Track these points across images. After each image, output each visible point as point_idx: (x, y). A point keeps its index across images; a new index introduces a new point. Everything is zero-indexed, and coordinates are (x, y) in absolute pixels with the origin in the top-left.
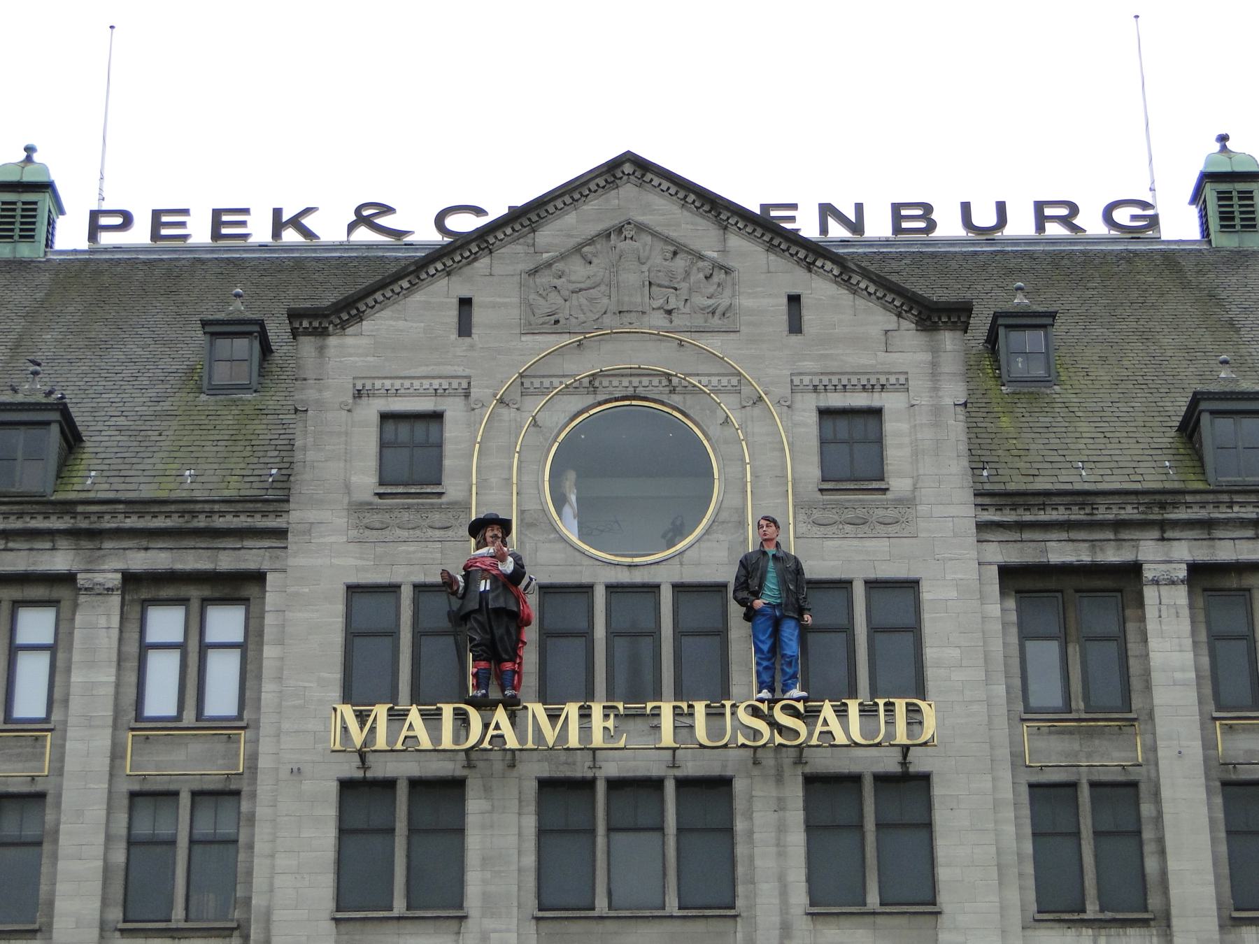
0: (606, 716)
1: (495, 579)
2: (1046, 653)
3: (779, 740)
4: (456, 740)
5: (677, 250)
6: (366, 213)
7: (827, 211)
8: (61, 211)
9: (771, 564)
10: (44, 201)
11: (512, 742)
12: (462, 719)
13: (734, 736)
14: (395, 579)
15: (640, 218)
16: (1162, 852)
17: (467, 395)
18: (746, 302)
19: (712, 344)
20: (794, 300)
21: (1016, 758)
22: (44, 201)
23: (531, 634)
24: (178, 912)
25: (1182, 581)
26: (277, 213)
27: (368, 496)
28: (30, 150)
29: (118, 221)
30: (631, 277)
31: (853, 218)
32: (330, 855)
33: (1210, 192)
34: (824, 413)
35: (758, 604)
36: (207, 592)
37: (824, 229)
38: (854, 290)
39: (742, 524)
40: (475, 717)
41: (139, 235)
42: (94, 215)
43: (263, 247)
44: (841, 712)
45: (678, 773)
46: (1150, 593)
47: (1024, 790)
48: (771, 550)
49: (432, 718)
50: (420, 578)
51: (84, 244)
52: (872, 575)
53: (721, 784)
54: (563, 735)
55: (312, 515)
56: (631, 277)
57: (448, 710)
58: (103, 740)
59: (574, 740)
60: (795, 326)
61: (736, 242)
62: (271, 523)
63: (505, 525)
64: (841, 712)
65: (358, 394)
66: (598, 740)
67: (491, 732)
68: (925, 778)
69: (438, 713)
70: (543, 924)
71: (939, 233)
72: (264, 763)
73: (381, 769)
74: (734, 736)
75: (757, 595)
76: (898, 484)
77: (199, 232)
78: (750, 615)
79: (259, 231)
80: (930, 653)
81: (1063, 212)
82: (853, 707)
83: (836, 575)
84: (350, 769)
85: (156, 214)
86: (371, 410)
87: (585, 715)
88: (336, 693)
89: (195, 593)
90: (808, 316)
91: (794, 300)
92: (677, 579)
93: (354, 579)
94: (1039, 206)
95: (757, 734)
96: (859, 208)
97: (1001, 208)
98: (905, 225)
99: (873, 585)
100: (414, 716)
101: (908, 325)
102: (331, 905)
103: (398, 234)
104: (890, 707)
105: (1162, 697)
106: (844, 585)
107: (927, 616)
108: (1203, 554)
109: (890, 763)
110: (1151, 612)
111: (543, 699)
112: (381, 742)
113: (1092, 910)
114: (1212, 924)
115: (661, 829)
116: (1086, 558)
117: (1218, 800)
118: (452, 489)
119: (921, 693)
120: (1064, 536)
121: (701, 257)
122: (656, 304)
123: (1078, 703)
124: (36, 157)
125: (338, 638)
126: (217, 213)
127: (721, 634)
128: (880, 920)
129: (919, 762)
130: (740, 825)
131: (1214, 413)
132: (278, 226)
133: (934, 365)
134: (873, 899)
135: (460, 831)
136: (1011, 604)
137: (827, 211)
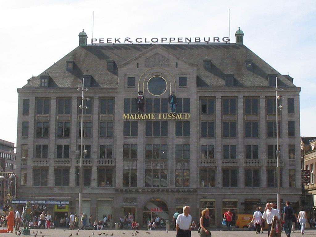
0: (153, 115)
1: (141, 99)
4: (137, 118)
6: (127, 39)
7: (186, 38)
8: (87, 37)
12: (137, 115)
14: (130, 98)
17: (138, 75)
19: (166, 69)
20: (177, 63)
21: (200, 119)
22: (86, 37)
23: (145, 105)
26: (115, 39)
28: (83, 30)
30: (157, 60)
31: (190, 40)
34: (180, 77)
35: (171, 102)
42: (92, 39)
44: (179, 115)
46: (217, 100)
47: (201, 123)
49: (134, 116)
51: (91, 44)
52: (184, 98)
54: (148, 117)
56: (157, 60)
57: (136, 114)
59: (149, 118)
60: (177, 67)
61: (170, 56)
62: (115, 91)
63: (142, 92)
64: (179, 115)
66: (152, 118)
67: (140, 117)
75: (171, 101)
76: (188, 86)
79: (113, 42)
80: (191, 107)
81: (217, 39)
82: (181, 114)
88: (123, 112)
91: (177, 63)
93: (125, 98)
97: (209, 38)
99: (184, 99)
103: (131, 42)
105: (217, 112)
106: (182, 99)
108: (223, 95)
109: (186, 121)
110: (217, 102)
111: (146, 113)
117: (223, 124)
132: (116, 41)
135: (137, 127)
136: (201, 101)
137: (186, 38)
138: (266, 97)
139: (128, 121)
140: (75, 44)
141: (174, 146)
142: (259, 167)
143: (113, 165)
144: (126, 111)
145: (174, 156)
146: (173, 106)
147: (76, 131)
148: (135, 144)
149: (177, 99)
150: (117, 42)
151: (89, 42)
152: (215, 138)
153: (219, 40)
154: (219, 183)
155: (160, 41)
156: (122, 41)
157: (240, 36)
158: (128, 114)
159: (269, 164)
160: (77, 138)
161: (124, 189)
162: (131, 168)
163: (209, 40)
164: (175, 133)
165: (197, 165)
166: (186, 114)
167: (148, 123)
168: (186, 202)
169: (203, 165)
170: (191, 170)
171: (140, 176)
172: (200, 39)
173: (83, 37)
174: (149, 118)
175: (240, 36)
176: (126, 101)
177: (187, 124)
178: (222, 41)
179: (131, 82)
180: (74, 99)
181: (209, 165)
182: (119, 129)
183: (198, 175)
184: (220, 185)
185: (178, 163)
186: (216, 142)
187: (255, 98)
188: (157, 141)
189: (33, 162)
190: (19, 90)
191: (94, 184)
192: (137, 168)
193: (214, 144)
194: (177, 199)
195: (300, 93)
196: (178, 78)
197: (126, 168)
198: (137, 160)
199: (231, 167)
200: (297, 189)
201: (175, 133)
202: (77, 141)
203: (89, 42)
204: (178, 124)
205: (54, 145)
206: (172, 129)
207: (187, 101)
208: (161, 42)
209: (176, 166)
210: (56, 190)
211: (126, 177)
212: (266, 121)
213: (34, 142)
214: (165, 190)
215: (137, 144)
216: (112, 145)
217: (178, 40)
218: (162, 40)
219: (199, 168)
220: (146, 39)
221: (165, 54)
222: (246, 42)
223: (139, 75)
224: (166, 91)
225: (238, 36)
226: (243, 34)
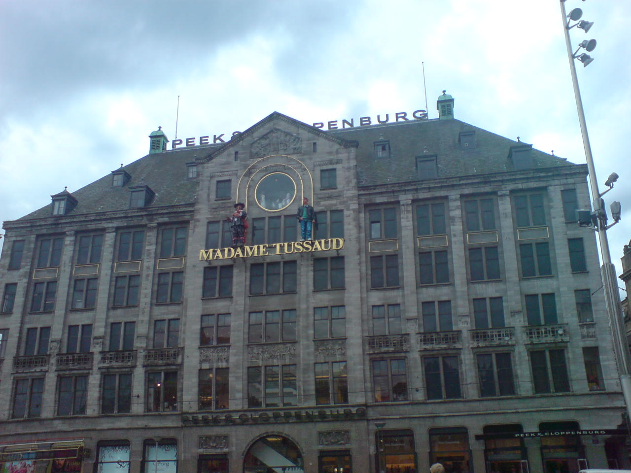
0: (264, 248)
1: (238, 217)
3: (305, 250)
7: (344, 121)
10: (162, 139)
12: (229, 250)
13: (294, 251)
15: (278, 127)
22: (162, 139)
24: (169, 300)
25: (410, 204)
26: (215, 136)
28: (160, 127)
29: (179, 142)
31: (351, 123)
36: (177, 226)
40: (233, 250)
41: (184, 145)
43: (212, 145)
44: (320, 243)
45: (284, 260)
47: (369, 258)
49: (223, 252)
53: (294, 262)
54: (253, 253)
59: (256, 254)
64: (320, 243)
66: (261, 254)
67: (237, 254)
68: (343, 258)
69: (224, 250)
70: (251, 298)
71: (372, 124)
73: (214, 264)
74: (294, 251)
77: (197, 143)
81: (403, 115)
82: (323, 241)
84: (206, 265)
85: (187, 140)
87: (259, 248)
94: (397, 114)
95: (299, 249)
96: (352, 120)
97: (387, 116)
100: (219, 251)
104: (332, 241)
109: (335, 254)
113: (385, 286)
117: (418, 258)
120: (380, 196)
122: (282, 148)
124: (161, 129)
125: (205, 234)
126: (201, 138)
127: (295, 227)
128: (331, 292)
129: (342, 253)
130: (298, 271)
131: (421, 161)
134: (329, 287)
135: (232, 277)
136: (368, 214)
137: (344, 121)
138: (512, 192)
140: (142, 149)
141: (311, 312)
142: (508, 345)
144: (209, 244)
145: (311, 332)
147: (107, 296)
149: (316, 213)
152: (402, 288)
158: (211, 250)
159: (532, 337)
160: (108, 309)
161: (200, 417)
162: (215, 366)
165: (364, 350)
166: (334, 240)
167: (256, 267)
168: (343, 440)
170: (350, 363)
171: (237, 384)
172: (371, 120)
174: (256, 254)
175: (448, 103)
177: (339, 259)
182: (193, 285)
183: (368, 373)
184: (420, 396)
186: (403, 296)
188: (274, 303)
190: (7, 225)
191: (137, 407)
192: (231, 365)
193: (399, 301)
194: (321, 434)
196: (318, 172)
197: (206, 366)
200: (609, 394)
201: (311, 283)
202: (107, 315)
204: (318, 261)
205: (61, 326)
206: (306, 276)
207: (337, 212)
210: (59, 425)
211: (204, 388)
212: (515, 242)
214: (293, 412)
215: (230, 312)
216: (178, 319)
219: (367, 358)
222: (460, 113)
225: (443, 104)
226: (452, 100)
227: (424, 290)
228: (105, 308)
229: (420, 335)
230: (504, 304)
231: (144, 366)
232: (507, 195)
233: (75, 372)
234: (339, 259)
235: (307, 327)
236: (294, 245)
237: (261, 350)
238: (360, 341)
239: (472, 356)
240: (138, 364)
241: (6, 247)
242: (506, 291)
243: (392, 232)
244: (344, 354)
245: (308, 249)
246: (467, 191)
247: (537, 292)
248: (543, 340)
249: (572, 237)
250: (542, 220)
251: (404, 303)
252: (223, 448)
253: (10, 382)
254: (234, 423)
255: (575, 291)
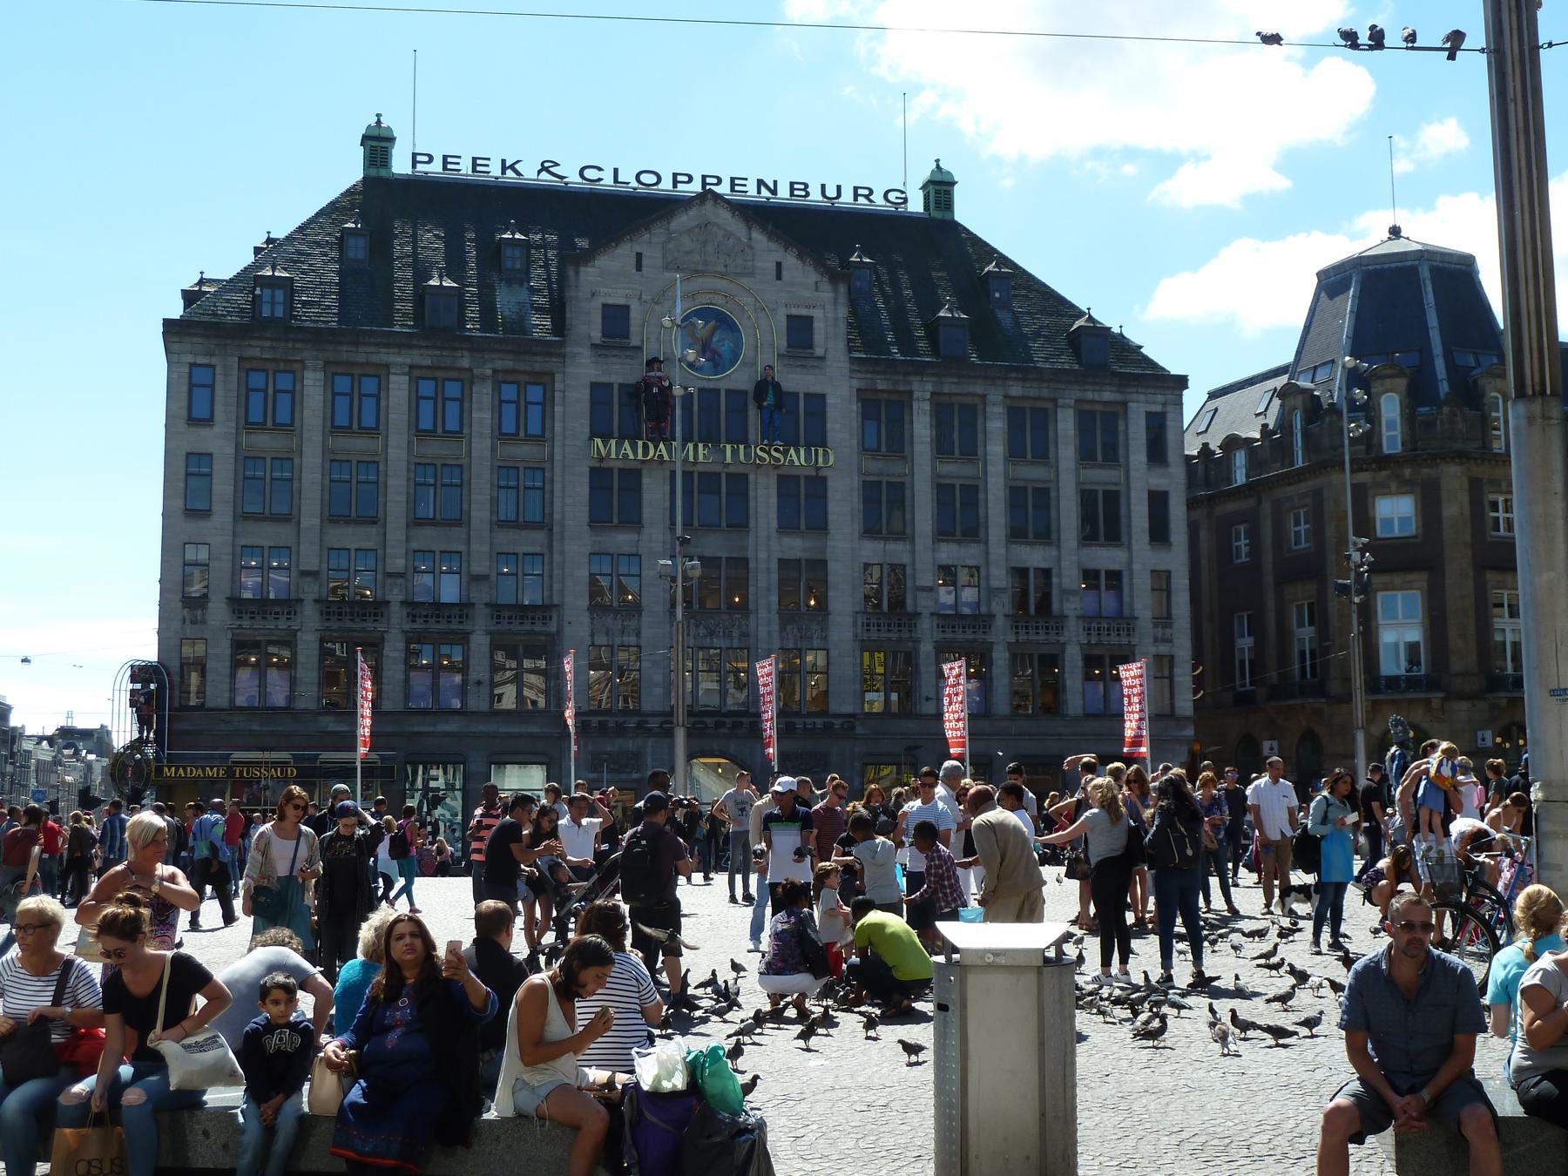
2: (871, 426)
5: (728, 235)
6: (546, 165)
7: (760, 183)
9: (770, 388)
11: (666, 458)
12: (645, 447)
16: (913, 512)
17: (640, 298)
18: (758, 264)
19: (745, 281)
20: (779, 265)
21: (860, 470)
26: (503, 161)
27: (598, 342)
31: (772, 187)
32: (587, 498)
33: (931, 189)
34: (789, 317)
35: (765, 404)
36: (526, 378)
37: (759, 192)
38: (804, 262)
39: (755, 364)
42: (414, 155)
46: (915, 405)
48: (770, 379)
49: (634, 449)
50: (621, 381)
51: (409, 171)
55: (576, 350)
56: (710, 249)
57: (640, 443)
58: (487, 443)
60: (779, 277)
62: (558, 351)
65: (593, 295)
66: (701, 458)
68: (825, 479)
72: (557, 457)
76: (819, 351)
78: (760, 407)
79: (495, 170)
80: (829, 426)
81: (866, 192)
83: (791, 390)
85: (445, 157)
86: (597, 304)
89: (523, 378)
90: (784, 273)
91: (779, 265)
92: (727, 387)
93: (594, 380)
95: (761, 458)
96: (775, 183)
97: (839, 188)
98: (796, 193)
99: (807, 395)
101: (826, 279)
102: (587, 520)
104: (816, 451)
105: (917, 448)
106: (796, 395)
107: (828, 410)
112: (613, 456)
114: (929, 541)
115: (719, 493)
116: (892, 388)
118: (634, 342)
119: (824, 444)
121: (740, 240)
123: (884, 448)
124: (382, 119)
125: (588, 405)
126: (474, 159)
127: (745, 411)
130: (751, 493)
133: (836, 299)
136: (860, 405)
137: (760, 183)
139: (604, 465)
141: (774, 565)
143: (554, 629)
144: (600, 429)
145: (775, 599)
146: (771, 417)
148: (633, 550)
150: (510, 173)
151: (400, 165)
153: (871, 197)
154: (928, 699)
155: (666, 184)
156: (529, 172)
157: (940, 188)
163: (839, 195)
164: (775, 516)
166: (821, 451)
169: (874, 635)
170: (833, 653)
173: (377, 144)
174: (691, 459)
175: (945, 188)
176: (599, 392)
178: (883, 202)
179: (616, 319)
180: (395, 374)
181: (894, 636)
185: (789, 627)
187: (1039, 404)
189: (234, 612)
192: (643, 642)
193: (906, 559)
195: (1185, 392)
198: (640, 615)
199: (967, 641)
201: (773, 515)
203: (400, 165)
204: (787, 483)
205: (317, 548)
206: (764, 499)
207: (817, 402)
208: (670, 187)
209: (782, 639)
213: (235, 534)
217: (733, 184)
218: (675, 183)
220: (616, 171)
221: (737, 227)
222: (967, 212)
223: (644, 297)
224: (744, 364)
225: (937, 188)
227: (944, 547)
228: (403, 522)
229: (935, 618)
230: (1055, 580)
231: (489, 633)
232: (1070, 407)
233: (355, 634)
234: (818, 484)
235: (769, 590)
236: (755, 453)
237: (692, 621)
238: (850, 620)
239: (1007, 655)
240: (476, 628)
241: (175, 375)
242: (1059, 560)
243: (897, 444)
244: (825, 638)
245: (778, 460)
246: (1016, 390)
247: (1099, 567)
248: (1105, 639)
249: (1154, 488)
250: (1113, 454)
251: (914, 563)
252: (630, 773)
253: (227, 644)
254: (649, 732)
255: (1152, 571)
